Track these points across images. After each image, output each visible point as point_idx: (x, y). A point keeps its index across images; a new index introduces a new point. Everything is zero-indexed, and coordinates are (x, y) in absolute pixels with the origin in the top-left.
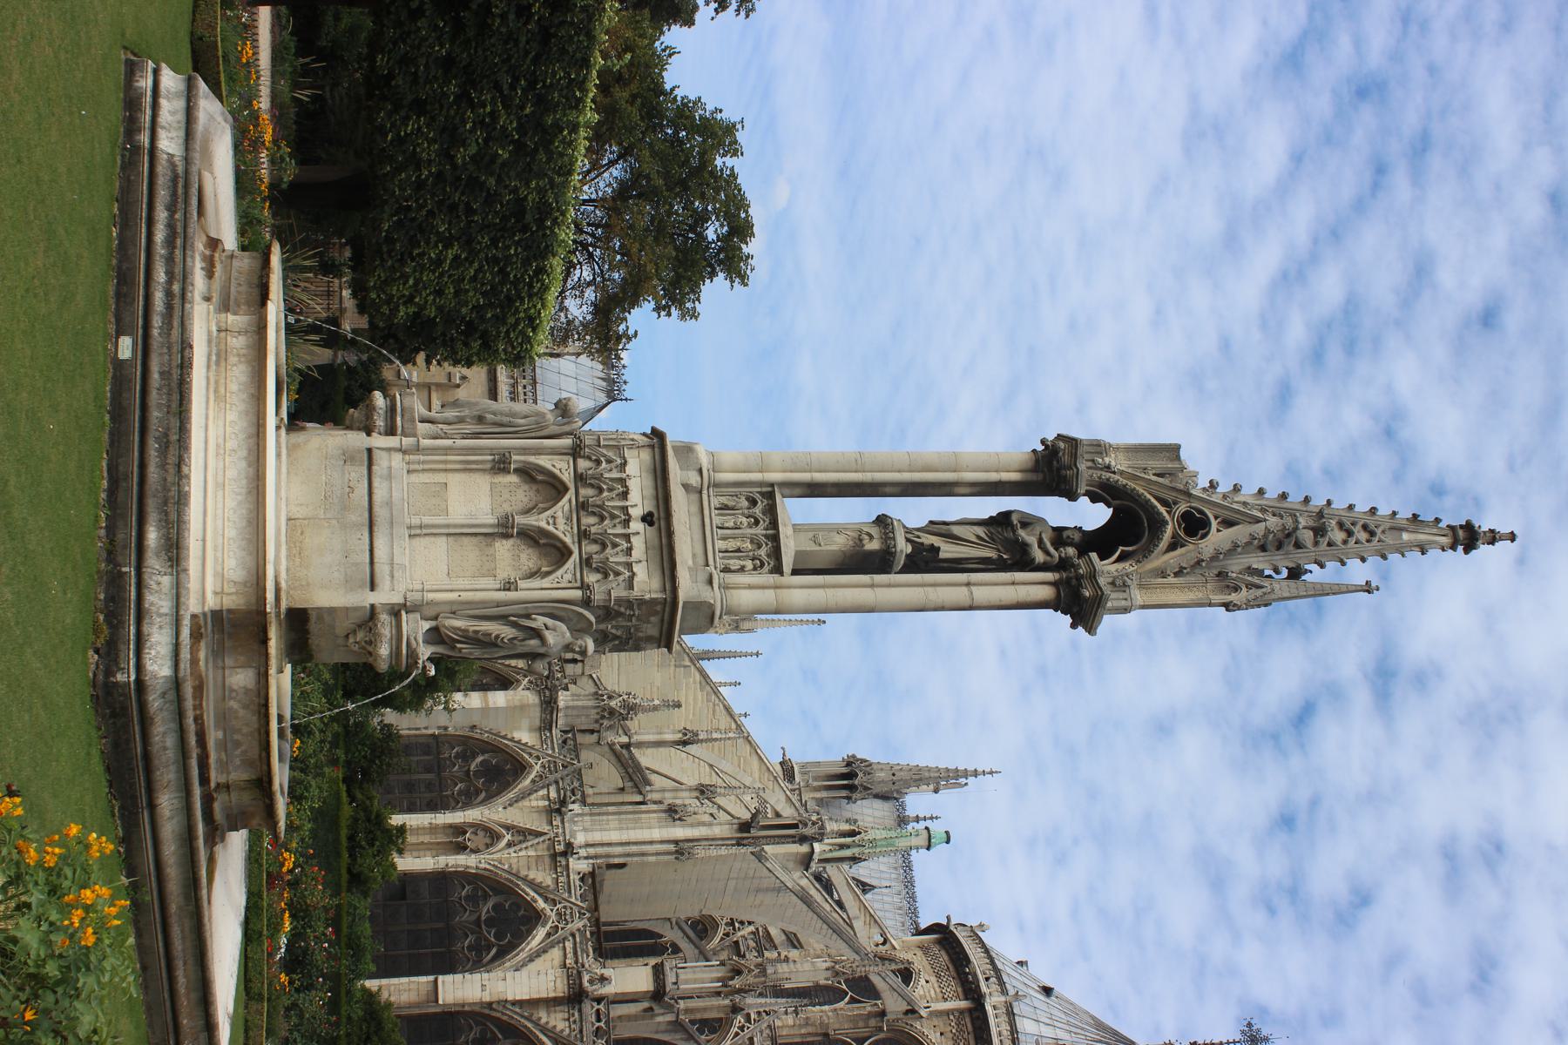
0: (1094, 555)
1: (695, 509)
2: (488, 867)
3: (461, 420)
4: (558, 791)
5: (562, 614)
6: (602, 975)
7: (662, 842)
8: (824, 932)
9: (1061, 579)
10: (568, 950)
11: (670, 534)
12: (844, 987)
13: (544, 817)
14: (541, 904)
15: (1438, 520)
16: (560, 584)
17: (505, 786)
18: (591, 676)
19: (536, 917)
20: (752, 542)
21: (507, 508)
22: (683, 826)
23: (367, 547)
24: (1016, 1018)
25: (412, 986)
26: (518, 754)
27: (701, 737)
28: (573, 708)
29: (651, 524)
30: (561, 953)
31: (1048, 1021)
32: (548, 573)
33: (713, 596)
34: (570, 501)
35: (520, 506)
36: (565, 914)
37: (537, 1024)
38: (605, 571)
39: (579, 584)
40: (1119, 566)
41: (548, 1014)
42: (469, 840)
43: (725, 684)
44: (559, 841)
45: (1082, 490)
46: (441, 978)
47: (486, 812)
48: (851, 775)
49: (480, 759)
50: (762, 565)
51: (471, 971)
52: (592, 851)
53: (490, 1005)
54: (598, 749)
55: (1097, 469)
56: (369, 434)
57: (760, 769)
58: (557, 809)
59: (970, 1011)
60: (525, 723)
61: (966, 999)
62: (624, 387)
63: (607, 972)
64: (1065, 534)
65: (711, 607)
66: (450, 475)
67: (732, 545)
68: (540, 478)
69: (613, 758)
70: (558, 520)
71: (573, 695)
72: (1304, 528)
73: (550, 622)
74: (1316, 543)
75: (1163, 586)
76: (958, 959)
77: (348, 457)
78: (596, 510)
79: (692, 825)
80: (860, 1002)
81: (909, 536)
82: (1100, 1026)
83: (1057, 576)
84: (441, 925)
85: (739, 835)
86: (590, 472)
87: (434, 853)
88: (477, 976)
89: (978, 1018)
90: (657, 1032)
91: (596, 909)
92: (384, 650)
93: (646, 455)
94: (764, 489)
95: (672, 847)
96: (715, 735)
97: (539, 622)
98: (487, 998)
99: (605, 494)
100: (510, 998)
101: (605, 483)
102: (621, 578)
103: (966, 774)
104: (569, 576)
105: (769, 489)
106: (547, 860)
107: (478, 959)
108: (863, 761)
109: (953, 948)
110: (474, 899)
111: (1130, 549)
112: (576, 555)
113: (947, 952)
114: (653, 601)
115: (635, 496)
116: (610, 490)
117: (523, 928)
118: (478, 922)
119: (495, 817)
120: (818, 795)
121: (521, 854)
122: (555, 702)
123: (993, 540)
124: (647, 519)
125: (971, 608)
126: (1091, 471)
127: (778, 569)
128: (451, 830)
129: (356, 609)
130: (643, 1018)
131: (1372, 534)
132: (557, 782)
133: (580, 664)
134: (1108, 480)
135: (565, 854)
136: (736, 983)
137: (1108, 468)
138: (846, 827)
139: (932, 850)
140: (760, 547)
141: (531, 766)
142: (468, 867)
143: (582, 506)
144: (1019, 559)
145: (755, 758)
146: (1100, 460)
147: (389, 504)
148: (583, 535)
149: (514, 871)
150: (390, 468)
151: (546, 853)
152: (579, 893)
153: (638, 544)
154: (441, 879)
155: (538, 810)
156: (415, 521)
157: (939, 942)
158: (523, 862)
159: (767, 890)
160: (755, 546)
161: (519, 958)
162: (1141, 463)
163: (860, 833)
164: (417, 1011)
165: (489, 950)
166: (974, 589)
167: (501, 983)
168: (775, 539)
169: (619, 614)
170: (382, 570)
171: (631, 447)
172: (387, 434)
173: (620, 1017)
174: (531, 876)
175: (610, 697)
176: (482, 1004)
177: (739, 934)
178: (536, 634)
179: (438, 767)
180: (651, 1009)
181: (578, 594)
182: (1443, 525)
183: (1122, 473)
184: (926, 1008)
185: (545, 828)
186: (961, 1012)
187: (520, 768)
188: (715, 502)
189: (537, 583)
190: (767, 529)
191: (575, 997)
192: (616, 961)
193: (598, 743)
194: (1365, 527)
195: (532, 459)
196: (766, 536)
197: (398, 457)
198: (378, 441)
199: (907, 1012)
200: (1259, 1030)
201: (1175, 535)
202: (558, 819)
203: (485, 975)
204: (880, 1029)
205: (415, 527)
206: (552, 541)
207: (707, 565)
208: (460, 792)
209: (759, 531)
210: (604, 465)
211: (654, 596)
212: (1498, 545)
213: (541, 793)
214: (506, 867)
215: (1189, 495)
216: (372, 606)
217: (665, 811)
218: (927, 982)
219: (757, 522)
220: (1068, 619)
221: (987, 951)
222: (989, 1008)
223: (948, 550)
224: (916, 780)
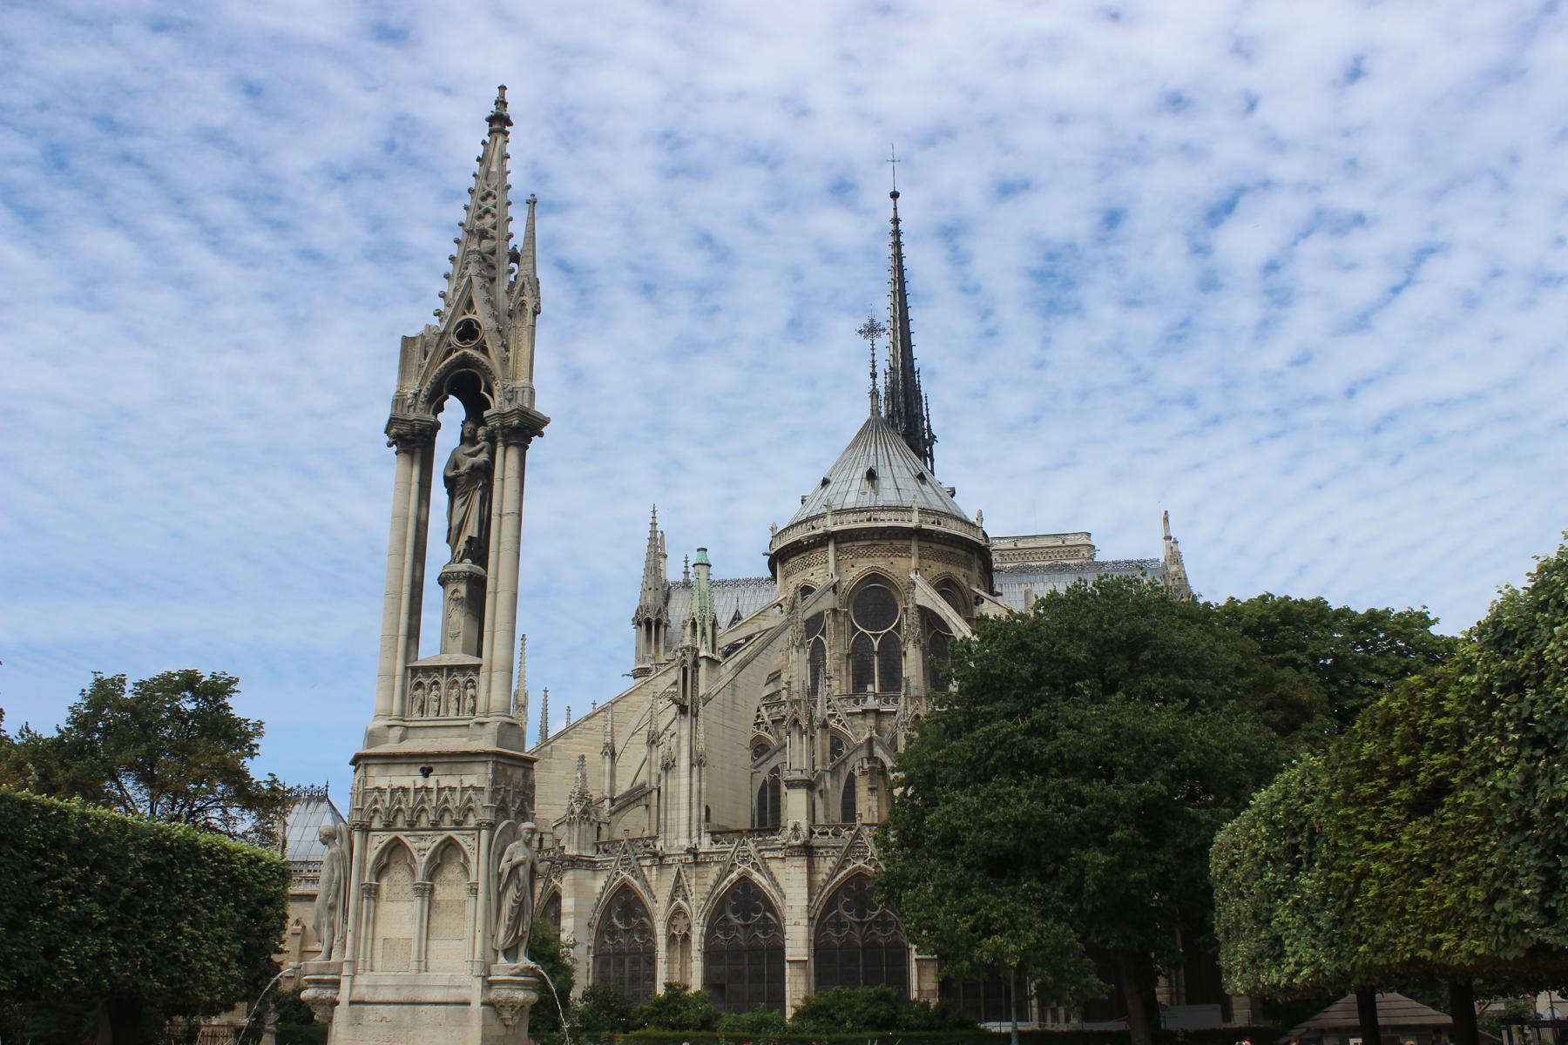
0: (486, 413)
1: (421, 733)
3: (331, 925)
4: (646, 858)
5: (499, 847)
7: (691, 776)
8: (769, 653)
9: (503, 442)
11: (440, 755)
12: (812, 639)
13: (666, 870)
14: (734, 876)
15: (484, 143)
16: (475, 847)
17: (639, 901)
18: (554, 827)
19: (744, 880)
20: (452, 688)
21: (409, 889)
22: (679, 759)
23: (434, 1007)
25: (793, 981)
26: (614, 889)
28: (579, 843)
29: (431, 770)
30: (773, 861)
31: (848, 484)
32: (466, 857)
33: (494, 723)
34: (406, 836)
35: (408, 877)
37: (827, 883)
38: (467, 810)
39: (476, 832)
40: (496, 394)
43: (568, 719)
45: (432, 418)
46: (788, 958)
48: (648, 623)
49: (615, 921)
50: (471, 681)
51: (783, 933)
52: (694, 833)
53: (810, 919)
54: (613, 824)
55: (416, 404)
57: (638, 695)
58: (660, 860)
59: (836, 543)
60: (589, 882)
62: (316, 787)
63: (790, 825)
64: (467, 435)
65: (502, 724)
67: (453, 705)
68: (385, 860)
69: (622, 813)
70: (422, 847)
71: (569, 842)
72: (479, 246)
73: (505, 857)
74: (493, 238)
75: (516, 361)
76: (796, 549)
77: (356, 1021)
78: (415, 814)
79: (679, 752)
81: (457, 560)
82: (854, 444)
83: (500, 444)
84: (746, 956)
86: (384, 818)
87: (689, 960)
88: (788, 929)
89: (842, 537)
90: (839, 788)
91: (740, 832)
92: (520, 995)
93: (373, 771)
94: (409, 675)
95: (695, 769)
96: (609, 729)
97: (505, 866)
98: (805, 921)
99: (403, 806)
101: (394, 806)
102: (474, 797)
103: (654, 532)
104: (469, 840)
105: (410, 671)
106: (700, 869)
107: (774, 928)
108: (637, 613)
109: (788, 552)
110: (727, 930)
111: (483, 384)
112: (452, 834)
114: (495, 772)
115: (407, 782)
116: (400, 802)
117: (752, 891)
118: (745, 927)
119: (663, 910)
120: (662, 650)
121: (693, 890)
122: (574, 857)
123: (466, 493)
124: (426, 772)
125: (520, 515)
126: (418, 410)
127: (476, 668)
128: (672, 947)
129: (484, 1018)
130: (827, 798)
131: (489, 194)
132: (638, 859)
133: (544, 836)
134: (426, 396)
135: (695, 855)
136: (804, 723)
137: (416, 395)
138: (689, 629)
139: (711, 563)
140: (457, 682)
141: (624, 879)
142: (701, 934)
143: (412, 826)
144: (484, 474)
145: (628, 698)
147: (398, 987)
148: (435, 826)
149: (707, 896)
150: (367, 986)
151: (694, 870)
152: (727, 845)
154: (710, 955)
155: (659, 875)
156: (414, 966)
158: (700, 889)
159: (733, 695)
160: (456, 686)
161: (775, 895)
162: (415, 368)
163: (694, 619)
164: (812, 978)
165: (768, 918)
166: (504, 512)
167: (794, 910)
168: (451, 669)
169: (503, 800)
170: (453, 995)
171: (365, 783)
172: (338, 988)
173: (825, 817)
174: (711, 882)
175: (572, 812)
177: (766, 719)
178: (515, 869)
179: (620, 955)
180: (821, 792)
181: (484, 833)
182: (488, 139)
183: (421, 385)
185: (674, 870)
186: (837, 550)
187: (625, 888)
188: (417, 716)
189: (473, 867)
193: (609, 824)
194: (483, 199)
195: (369, 866)
196: (448, 677)
197: (360, 980)
198: (344, 995)
199: (835, 592)
200: (865, 325)
201: (476, 348)
202: (667, 859)
203: (787, 922)
204: (846, 613)
205: (419, 966)
206: (439, 852)
208: (642, 938)
209: (443, 681)
210: (378, 806)
211: (490, 771)
212: (507, 99)
213: (646, 872)
214: (703, 903)
215: (444, 333)
216: (483, 1004)
217: (667, 773)
219: (436, 683)
220: (535, 439)
221: (792, 526)
222: (836, 528)
223: (472, 530)
224: (656, 572)
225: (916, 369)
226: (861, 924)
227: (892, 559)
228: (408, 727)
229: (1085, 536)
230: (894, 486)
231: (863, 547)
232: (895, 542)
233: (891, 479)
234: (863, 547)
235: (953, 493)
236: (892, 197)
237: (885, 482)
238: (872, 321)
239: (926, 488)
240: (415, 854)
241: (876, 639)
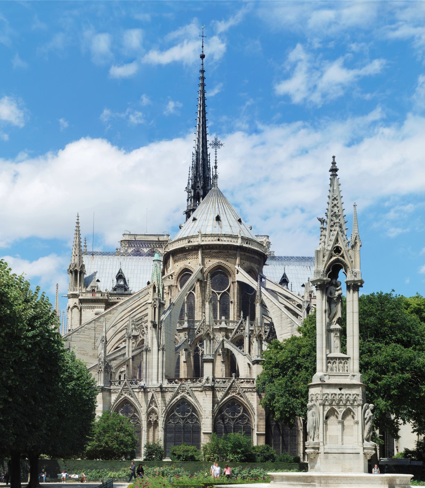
1: (333, 377)
2: (164, 414)
6: (206, 379)
14: (178, 397)
19: (183, 400)
24: (206, 234)
30: (196, 392)
32: (353, 413)
42: (153, 419)
44: (156, 390)
47: (143, 413)
52: (160, 379)
56: (318, 453)
59: (203, 250)
61: (198, 250)
66: (327, 435)
67: (341, 368)
77: (327, 458)
89: (205, 247)
95: (161, 352)
99: (335, 399)
113: (178, 254)
118: (183, 419)
124: (340, 389)
127: (348, 359)
140: (341, 362)
142: (163, 421)
143: (338, 405)
146: (322, 273)
148: (345, 405)
152: (175, 384)
154: (166, 429)
156: (341, 443)
168: (339, 358)
184: (200, 265)
186: (202, 253)
190: (337, 360)
191: (213, 389)
192: (181, 372)
195: (325, 415)
196: (339, 360)
199: (201, 272)
207: (348, 376)
209: (337, 361)
210: (327, 398)
218: (189, 263)
219: (335, 362)
227: (228, 259)
228: (329, 375)
229: (266, 237)
230: (228, 225)
231: (215, 252)
232: (230, 251)
233: (227, 221)
240: (339, 412)
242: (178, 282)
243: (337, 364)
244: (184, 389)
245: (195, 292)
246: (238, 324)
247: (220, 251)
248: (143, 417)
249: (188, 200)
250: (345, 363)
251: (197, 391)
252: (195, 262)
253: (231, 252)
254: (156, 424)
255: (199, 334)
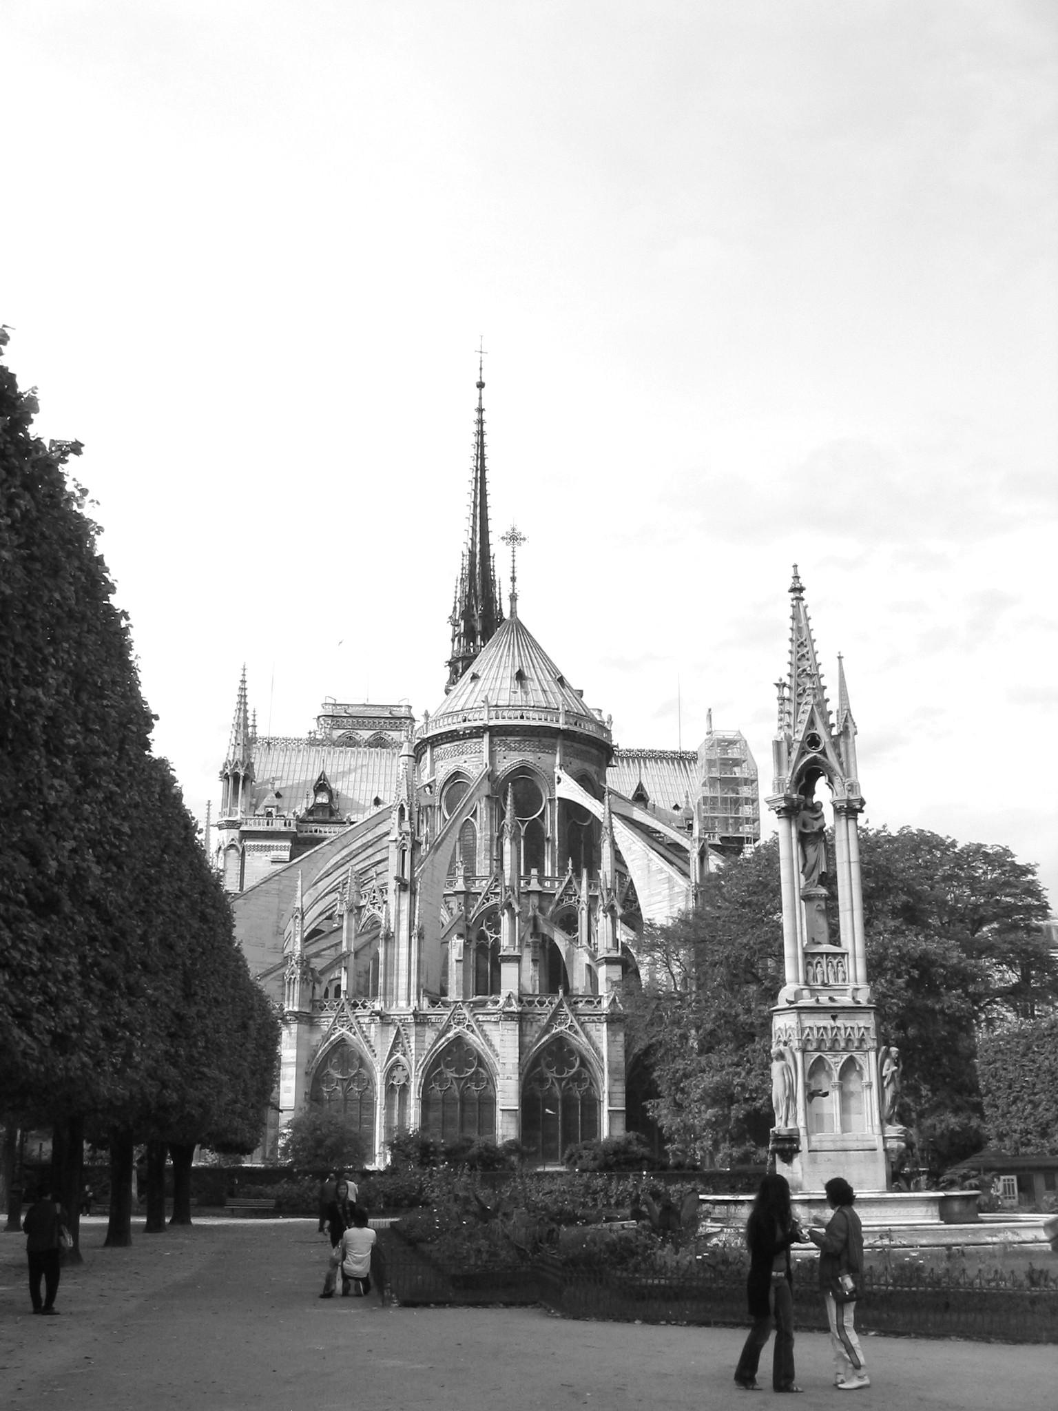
9: (846, 816)
10: (484, 1019)
14: (450, 1035)
19: (459, 1040)
27: (300, 906)
30: (486, 1023)
36: (459, 1019)
38: (862, 1040)
41: (527, 1035)
46: (499, 1107)
52: (413, 996)
53: (520, 1074)
61: (482, 737)
70: (836, 1062)
77: (814, 1161)
80: (476, 810)
85: (409, 892)
93: (803, 1016)
95: (415, 941)
99: (825, 1037)
100: (517, 1061)
104: (863, 1057)
108: (225, 766)
115: (821, 1023)
116: (822, 1035)
124: (834, 1018)
127: (843, 955)
132: (357, 1017)
138: (396, 815)
141: (342, 1034)
143: (830, 1050)
146: (788, 785)
148: (844, 1050)
153: (849, 1024)
157: (432, 748)
163: (402, 805)
168: (828, 954)
170: (867, 1145)
176: (520, 1079)
181: (872, 1054)
186: (491, 742)
195: (807, 1072)
201: (819, 752)
207: (846, 990)
209: (824, 962)
210: (810, 1037)
212: (799, 574)
218: (465, 762)
219: (819, 962)
222: (492, 723)
225: (491, 555)
226: (560, 1080)
227: (540, 755)
230: (539, 688)
231: (516, 742)
232: (544, 740)
234: (516, 742)
235: (581, 693)
236: (478, 387)
237: (532, 685)
238: (513, 530)
239: (566, 691)
240: (833, 1067)
241: (523, 825)
242: (443, 799)
243: (825, 966)
244: (462, 1017)
245: (476, 819)
246: (564, 884)
247: (525, 738)
248: (379, 1078)
249: (453, 640)
250: (840, 964)
251: (488, 1021)
252: (477, 759)
253: (546, 741)
254: (405, 1089)
255: (487, 905)
